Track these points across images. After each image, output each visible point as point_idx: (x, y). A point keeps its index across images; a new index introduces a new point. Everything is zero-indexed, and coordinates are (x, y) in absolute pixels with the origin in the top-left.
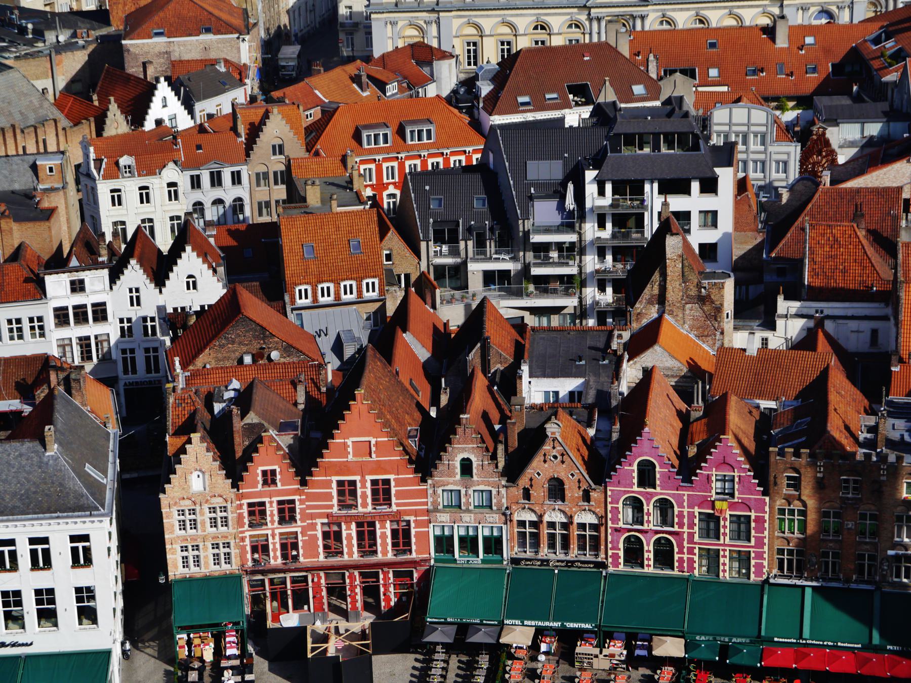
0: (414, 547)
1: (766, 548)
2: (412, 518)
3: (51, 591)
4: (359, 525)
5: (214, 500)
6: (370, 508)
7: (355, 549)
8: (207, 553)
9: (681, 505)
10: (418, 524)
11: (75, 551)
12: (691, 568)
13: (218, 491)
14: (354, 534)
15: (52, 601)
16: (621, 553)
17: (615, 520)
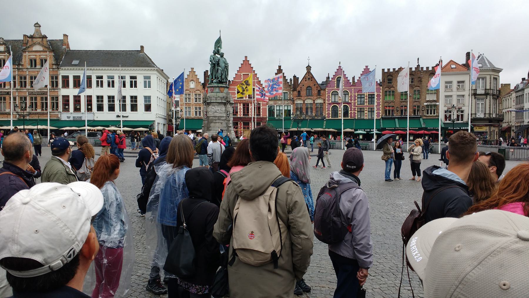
0: (261, 113)
1: (381, 106)
2: (261, 103)
3: (136, 97)
4: (244, 105)
5: (197, 92)
6: (247, 98)
7: (242, 113)
8: (193, 111)
9: (351, 93)
10: (263, 105)
11: (145, 82)
12: (355, 116)
13: (199, 88)
14: (242, 107)
15: (136, 101)
16: (330, 112)
17: (329, 100)
